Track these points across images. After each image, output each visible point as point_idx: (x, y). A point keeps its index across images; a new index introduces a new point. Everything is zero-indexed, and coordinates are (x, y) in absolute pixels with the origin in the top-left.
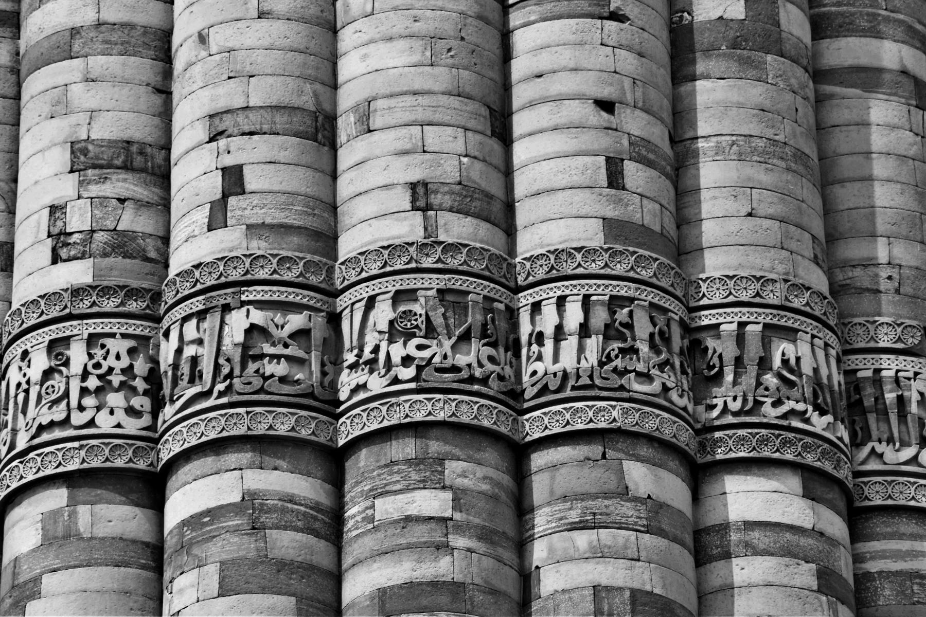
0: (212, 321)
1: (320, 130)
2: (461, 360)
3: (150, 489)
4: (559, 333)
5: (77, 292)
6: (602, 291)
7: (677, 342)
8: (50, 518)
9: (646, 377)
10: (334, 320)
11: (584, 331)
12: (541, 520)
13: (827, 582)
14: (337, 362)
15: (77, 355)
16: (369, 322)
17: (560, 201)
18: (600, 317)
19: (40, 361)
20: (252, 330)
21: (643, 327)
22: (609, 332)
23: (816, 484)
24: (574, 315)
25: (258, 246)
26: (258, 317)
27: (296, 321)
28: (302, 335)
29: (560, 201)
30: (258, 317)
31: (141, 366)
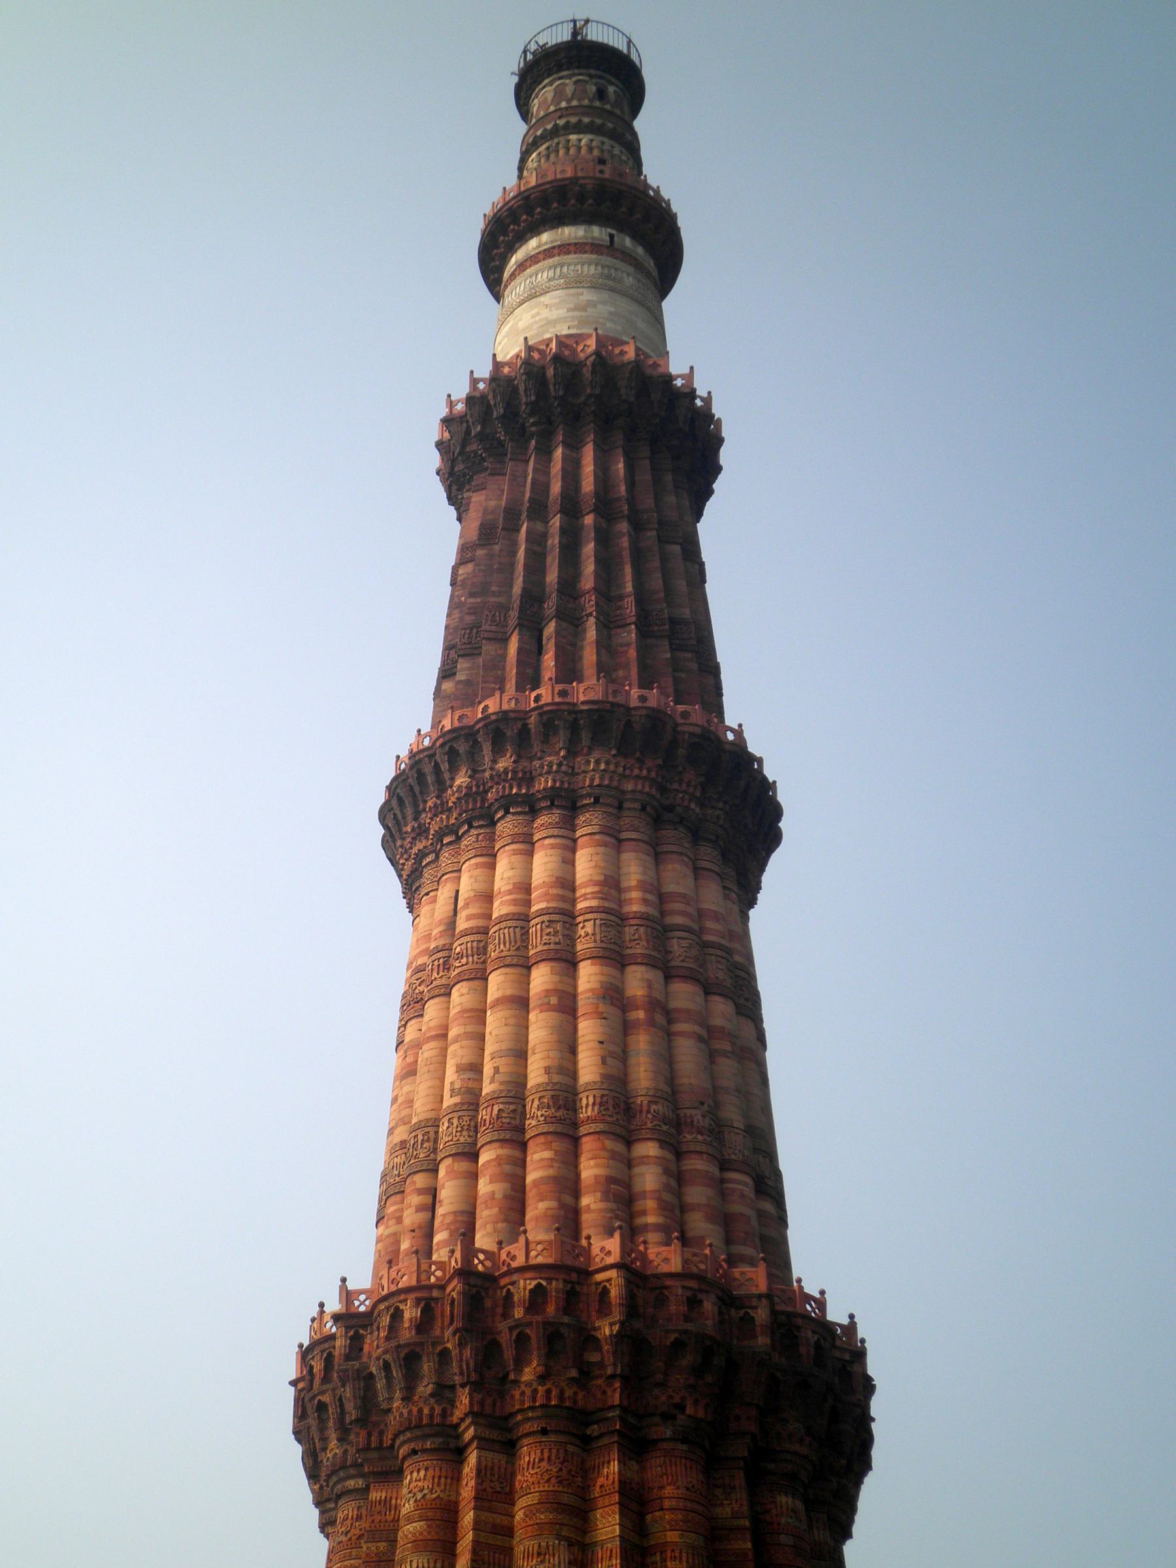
0: (489, 1109)
1: (520, 1054)
2: (557, 1114)
3: (474, 1157)
4: (587, 1105)
5: (456, 1105)
6: (598, 1093)
7: (622, 1105)
8: (447, 1167)
9: (611, 1116)
10: (524, 1106)
11: (594, 1104)
12: (583, 1159)
13: (666, 1172)
14: (525, 1119)
15: (455, 1122)
16: (533, 1107)
17: (588, 1068)
18: (598, 1100)
19: (446, 1124)
20: (500, 1110)
21: (611, 1102)
22: (601, 1104)
23: (663, 1144)
24: (591, 1100)
25: (502, 1088)
26: (501, 1106)
27: (512, 1107)
28: (514, 1111)
29: (588, 1068)
30: (501, 1106)
31: (472, 1124)
